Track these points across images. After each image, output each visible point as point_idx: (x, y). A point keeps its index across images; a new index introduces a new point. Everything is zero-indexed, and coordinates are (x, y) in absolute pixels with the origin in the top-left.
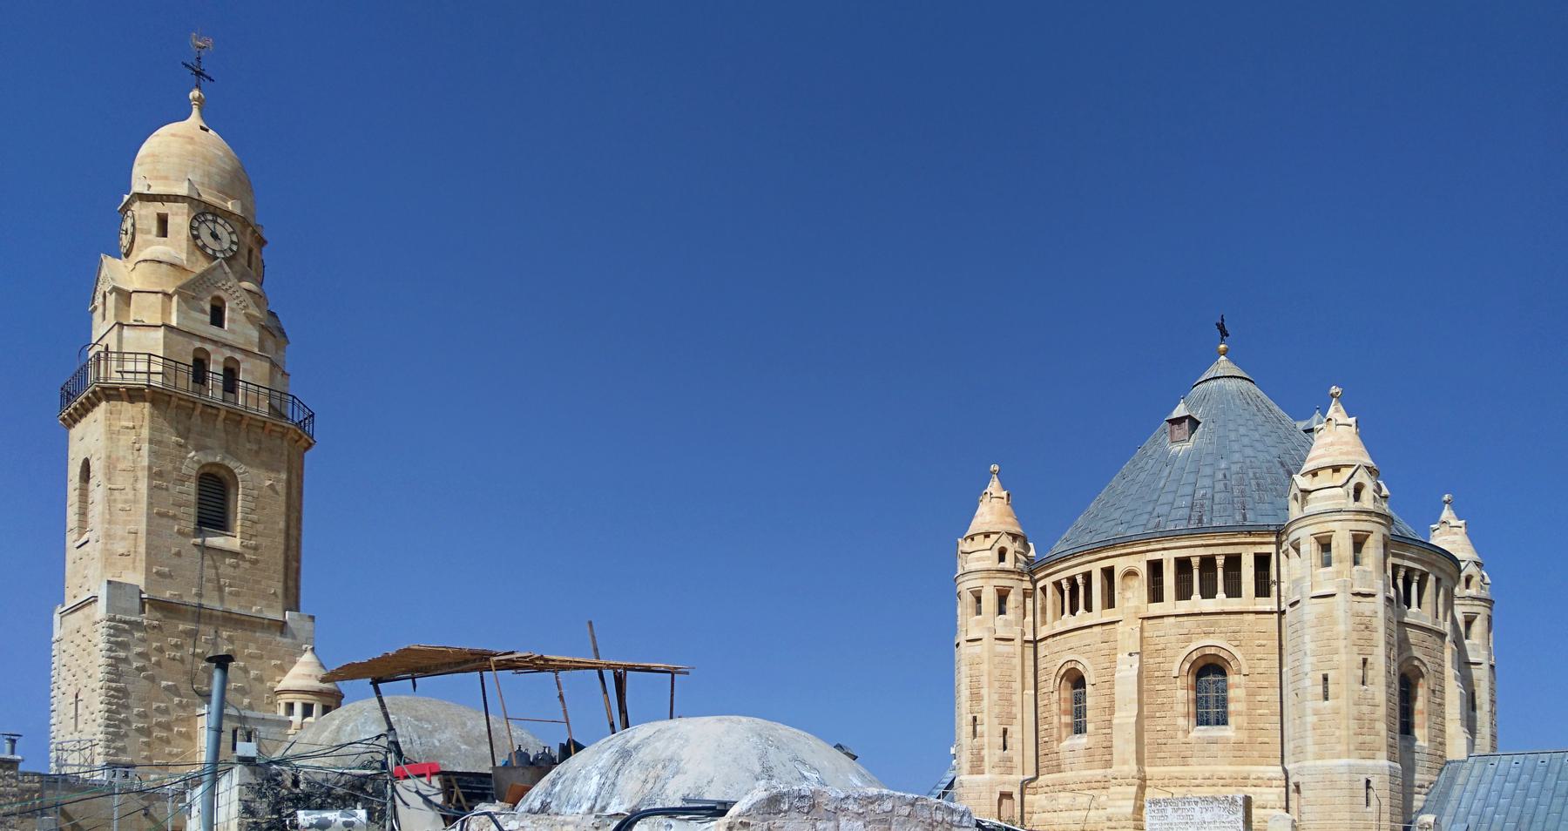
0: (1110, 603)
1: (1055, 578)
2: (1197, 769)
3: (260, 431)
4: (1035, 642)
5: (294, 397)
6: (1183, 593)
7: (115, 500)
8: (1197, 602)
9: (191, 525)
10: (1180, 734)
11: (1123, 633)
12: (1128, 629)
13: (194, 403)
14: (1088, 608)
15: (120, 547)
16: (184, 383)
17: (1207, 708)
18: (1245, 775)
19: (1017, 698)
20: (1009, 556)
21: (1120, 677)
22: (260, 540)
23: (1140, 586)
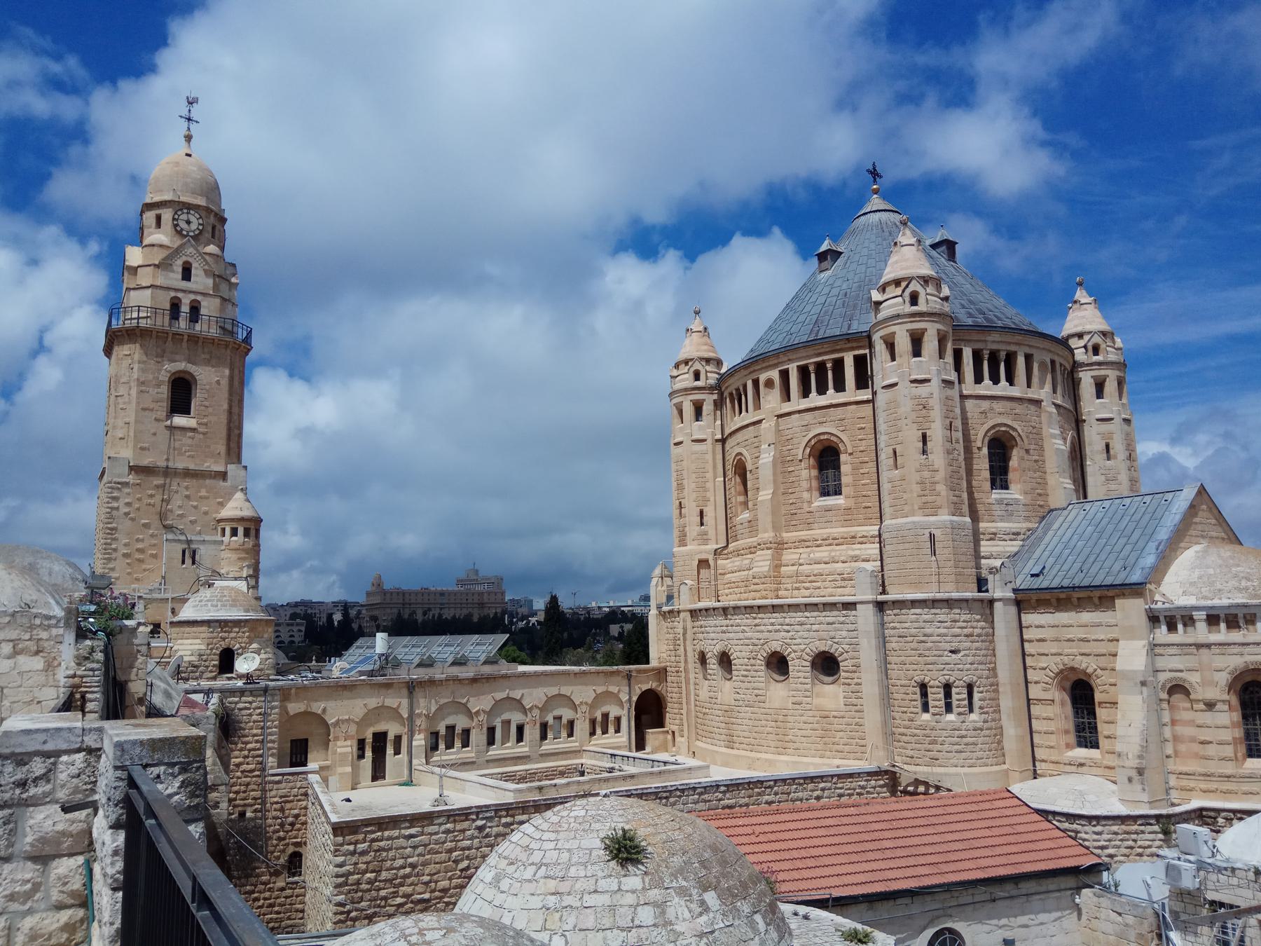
0: (758, 406)
1: (729, 390)
2: (818, 532)
3: (211, 345)
4: (723, 441)
6: (805, 393)
8: (815, 399)
10: (805, 505)
11: (764, 428)
12: (767, 425)
13: (167, 333)
14: (747, 412)
16: (163, 322)
17: (828, 482)
18: (853, 534)
19: (710, 485)
20: (702, 376)
21: (763, 464)
22: (210, 418)
23: (776, 392)
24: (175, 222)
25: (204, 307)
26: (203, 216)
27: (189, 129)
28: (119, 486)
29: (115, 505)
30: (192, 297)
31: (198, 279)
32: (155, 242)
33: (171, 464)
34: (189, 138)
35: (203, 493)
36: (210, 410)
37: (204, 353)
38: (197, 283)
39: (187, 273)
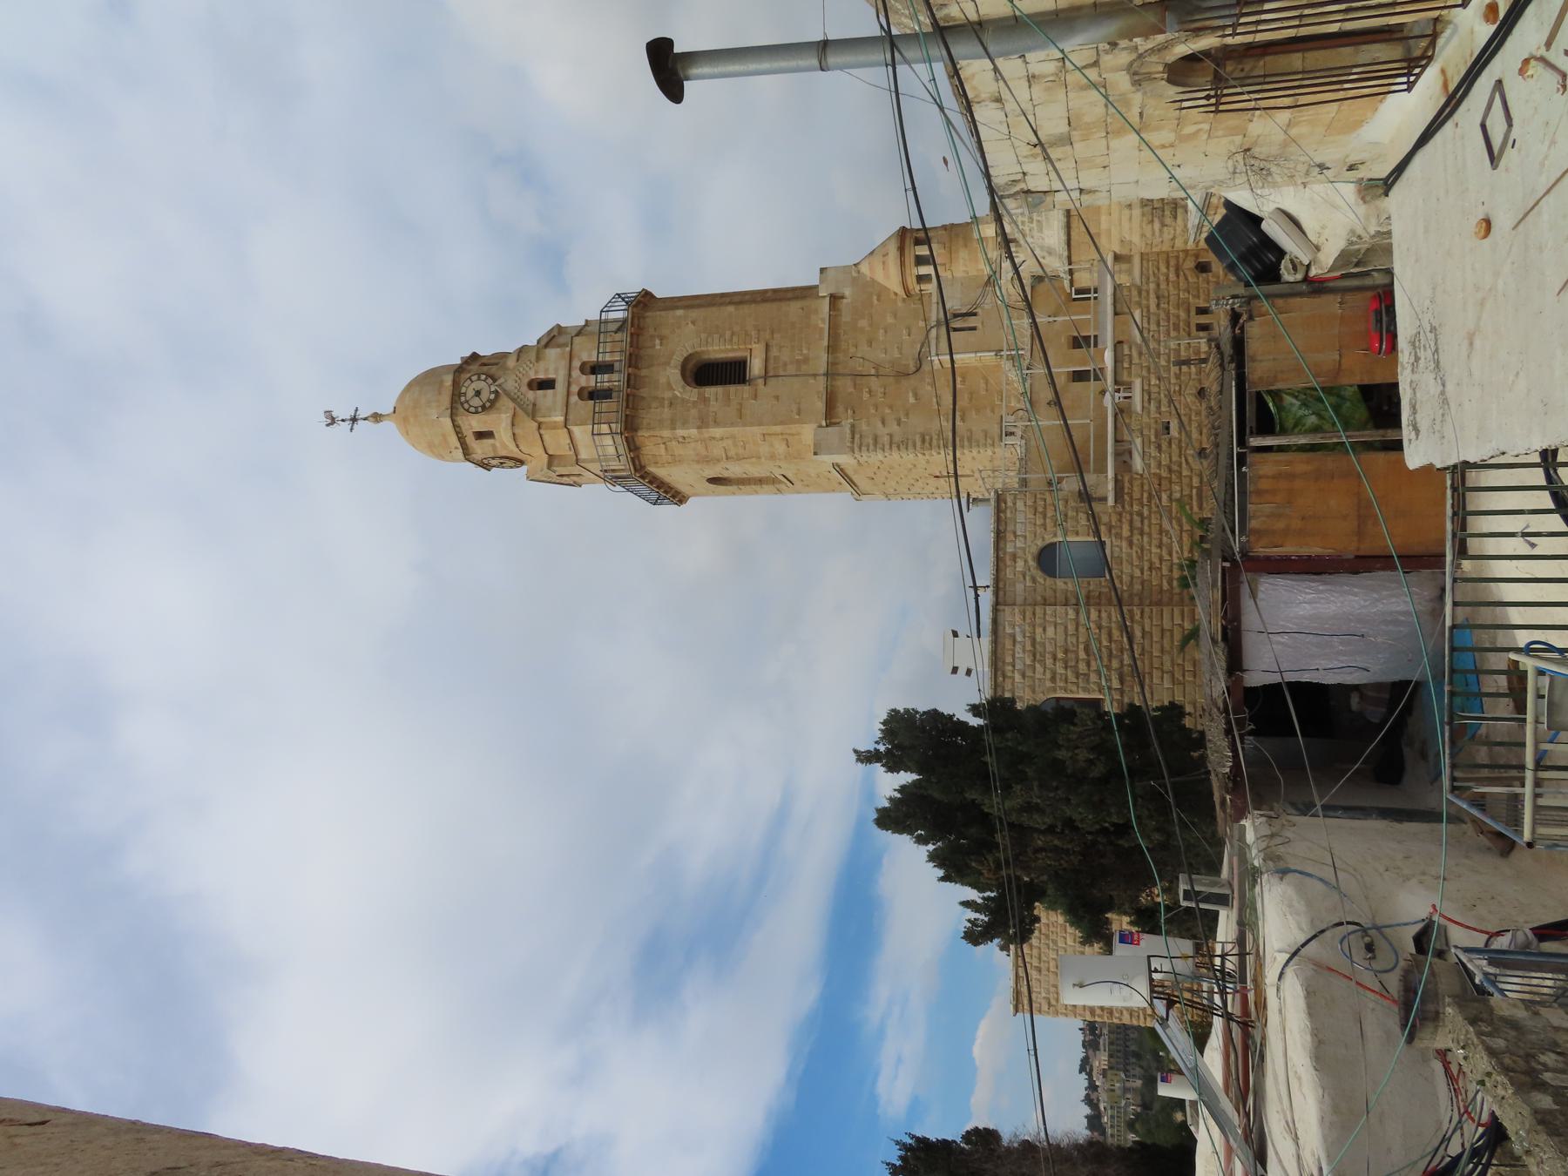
5: (602, 311)
7: (737, 454)
9: (745, 390)
15: (780, 448)
24: (480, 409)
25: (590, 356)
26: (469, 375)
27: (365, 419)
28: (857, 436)
29: (886, 439)
30: (576, 373)
31: (552, 367)
32: (510, 434)
33: (823, 370)
34: (377, 417)
35: (863, 323)
36: (736, 329)
37: (654, 346)
38: (556, 370)
39: (547, 384)
